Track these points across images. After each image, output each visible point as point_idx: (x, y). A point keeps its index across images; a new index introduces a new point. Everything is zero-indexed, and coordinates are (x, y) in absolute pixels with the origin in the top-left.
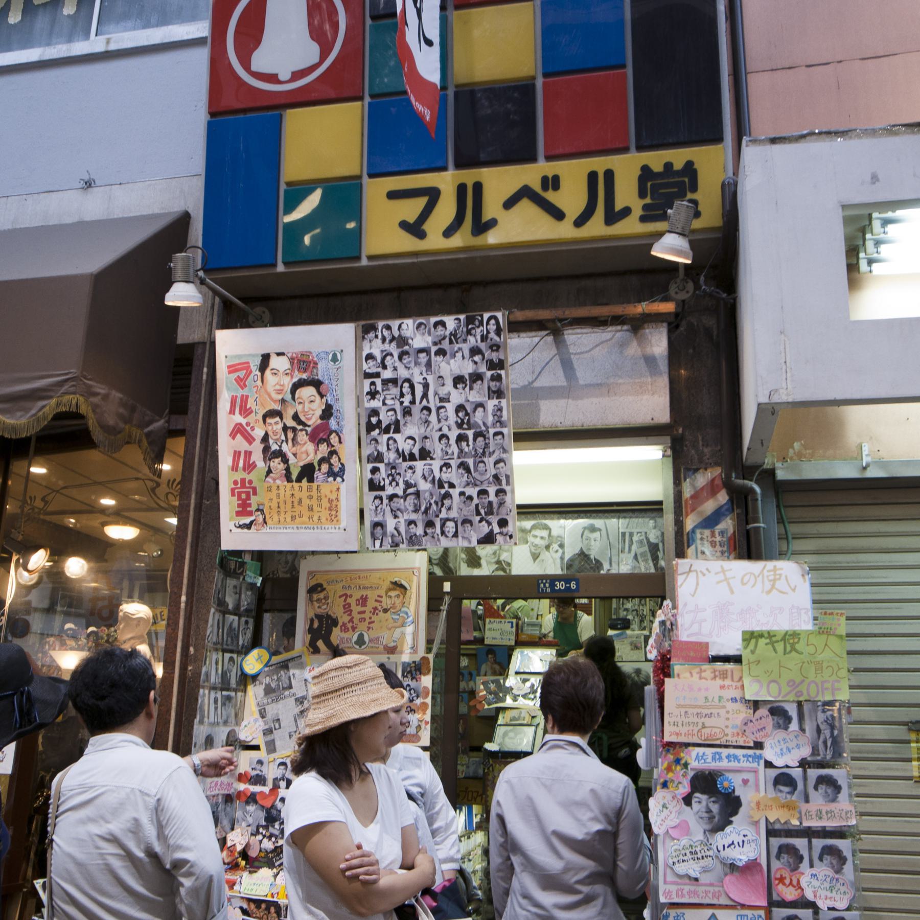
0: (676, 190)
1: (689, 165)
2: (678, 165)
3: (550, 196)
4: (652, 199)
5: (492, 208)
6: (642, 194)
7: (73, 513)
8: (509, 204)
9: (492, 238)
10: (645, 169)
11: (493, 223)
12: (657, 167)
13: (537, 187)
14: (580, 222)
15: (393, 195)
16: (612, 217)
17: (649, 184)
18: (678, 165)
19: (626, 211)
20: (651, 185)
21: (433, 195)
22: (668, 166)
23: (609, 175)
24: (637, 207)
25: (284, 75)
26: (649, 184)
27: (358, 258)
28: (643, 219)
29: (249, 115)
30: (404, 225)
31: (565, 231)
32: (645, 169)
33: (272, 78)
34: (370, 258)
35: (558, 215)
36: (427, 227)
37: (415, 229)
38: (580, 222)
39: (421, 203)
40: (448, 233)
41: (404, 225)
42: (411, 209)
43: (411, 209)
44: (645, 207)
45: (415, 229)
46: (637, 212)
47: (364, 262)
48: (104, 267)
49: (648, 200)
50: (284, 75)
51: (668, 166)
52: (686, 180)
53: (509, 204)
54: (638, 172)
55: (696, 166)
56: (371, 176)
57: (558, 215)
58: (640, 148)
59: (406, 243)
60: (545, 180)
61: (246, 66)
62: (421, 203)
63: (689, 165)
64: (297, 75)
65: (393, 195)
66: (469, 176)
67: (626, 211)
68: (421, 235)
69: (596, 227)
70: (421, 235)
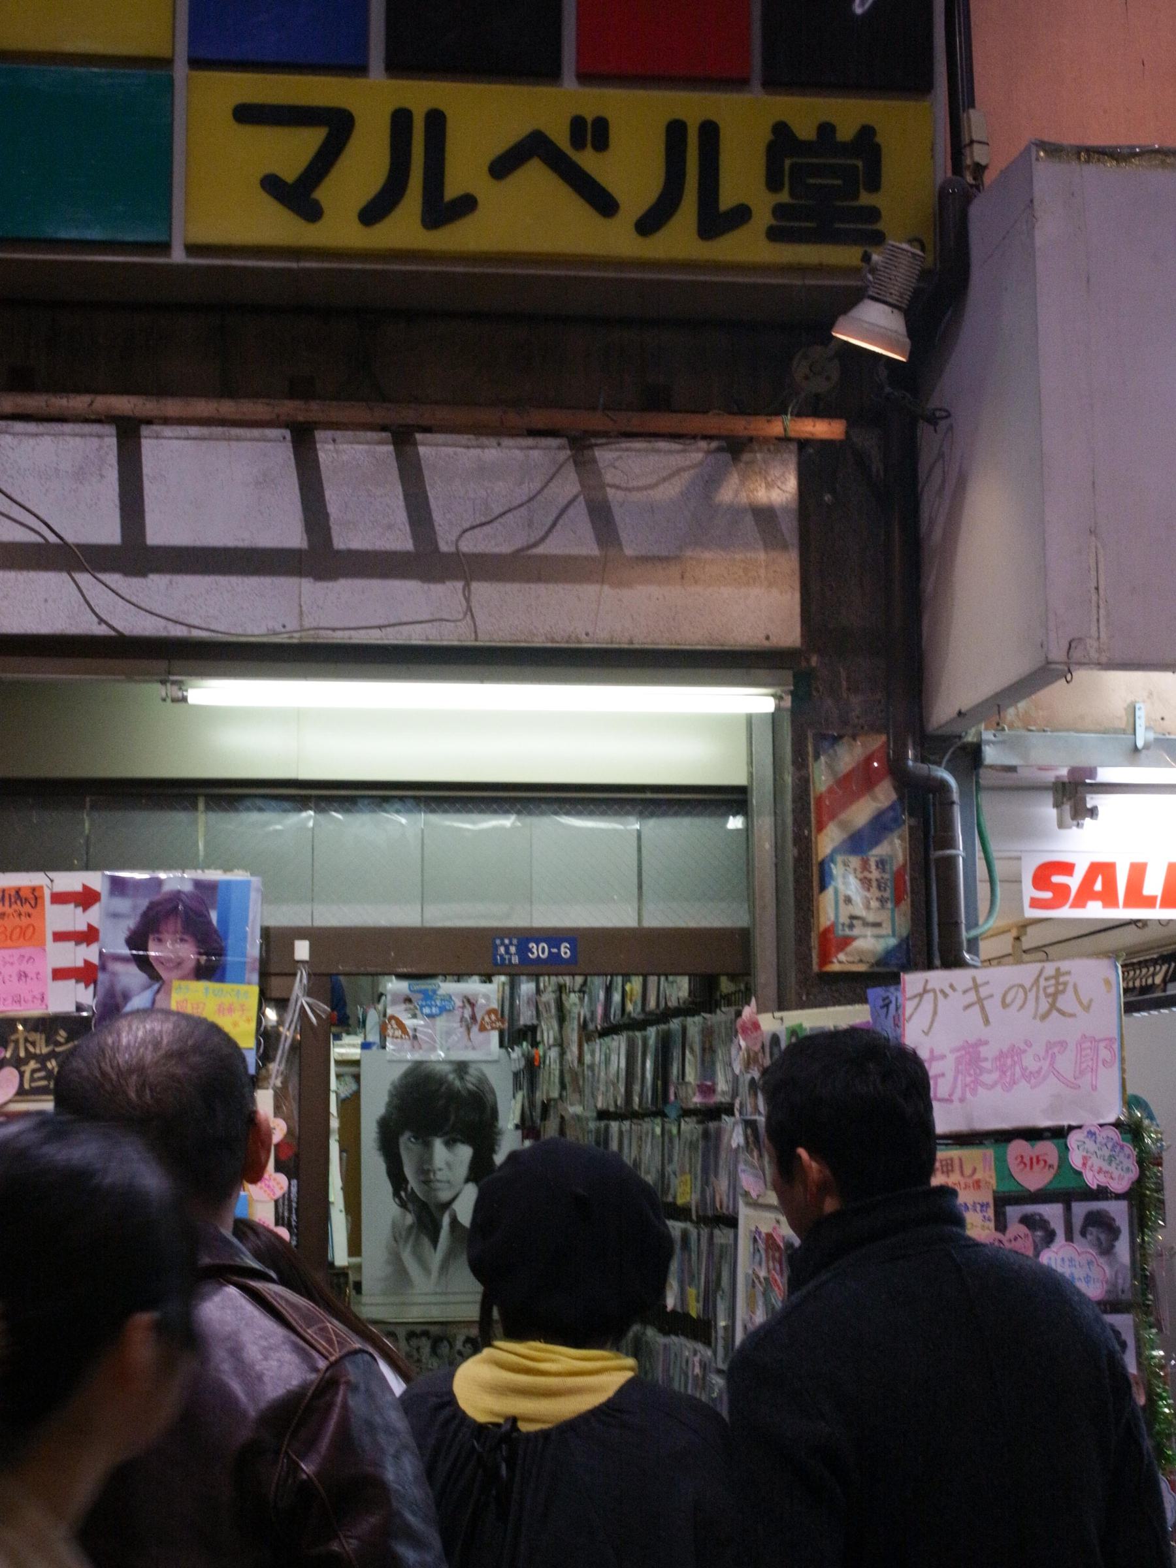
0: (839, 182)
1: (867, 132)
2: (846, 132)
3: (588, 160)
4: (792, 194)
6: (773, 183)
8: (502, 167)
10: (781, 130)
11: (467, 204)
12: (805, 131)
13: (561, 137)
14: (648, 224)
15: (247, 114)
17: (787, 163)
18: (846, 132)
19: (741, 214)
20: (792, 166)
22: (826, 130)
23: (710, 132)
24: (763, 205)
26: (787, 163)
27: (164, 247)
28: (774, 234)
30: (272, 185)
32: (781, 130)
34: (192, 249)
36: (323, 194)
38: (648, 224)
39: (311, 139)
40: (372, 214)
41: (272, 185)
44: (779, 211)
46: (762, 218)
47: (178, 256)
49: (784, 197)
51: (826, 130)
52: (860, 164)
53: (502, 167)
54: (768, 136)
55: (879, 139)
56: (196, 63)
58: (772, 84)
60: (578, 124)
62: (311, 139)
63: (867, 132)
65: (247, 114)
67: (741, 214)
68: (312, 213)
70: (312, 213)
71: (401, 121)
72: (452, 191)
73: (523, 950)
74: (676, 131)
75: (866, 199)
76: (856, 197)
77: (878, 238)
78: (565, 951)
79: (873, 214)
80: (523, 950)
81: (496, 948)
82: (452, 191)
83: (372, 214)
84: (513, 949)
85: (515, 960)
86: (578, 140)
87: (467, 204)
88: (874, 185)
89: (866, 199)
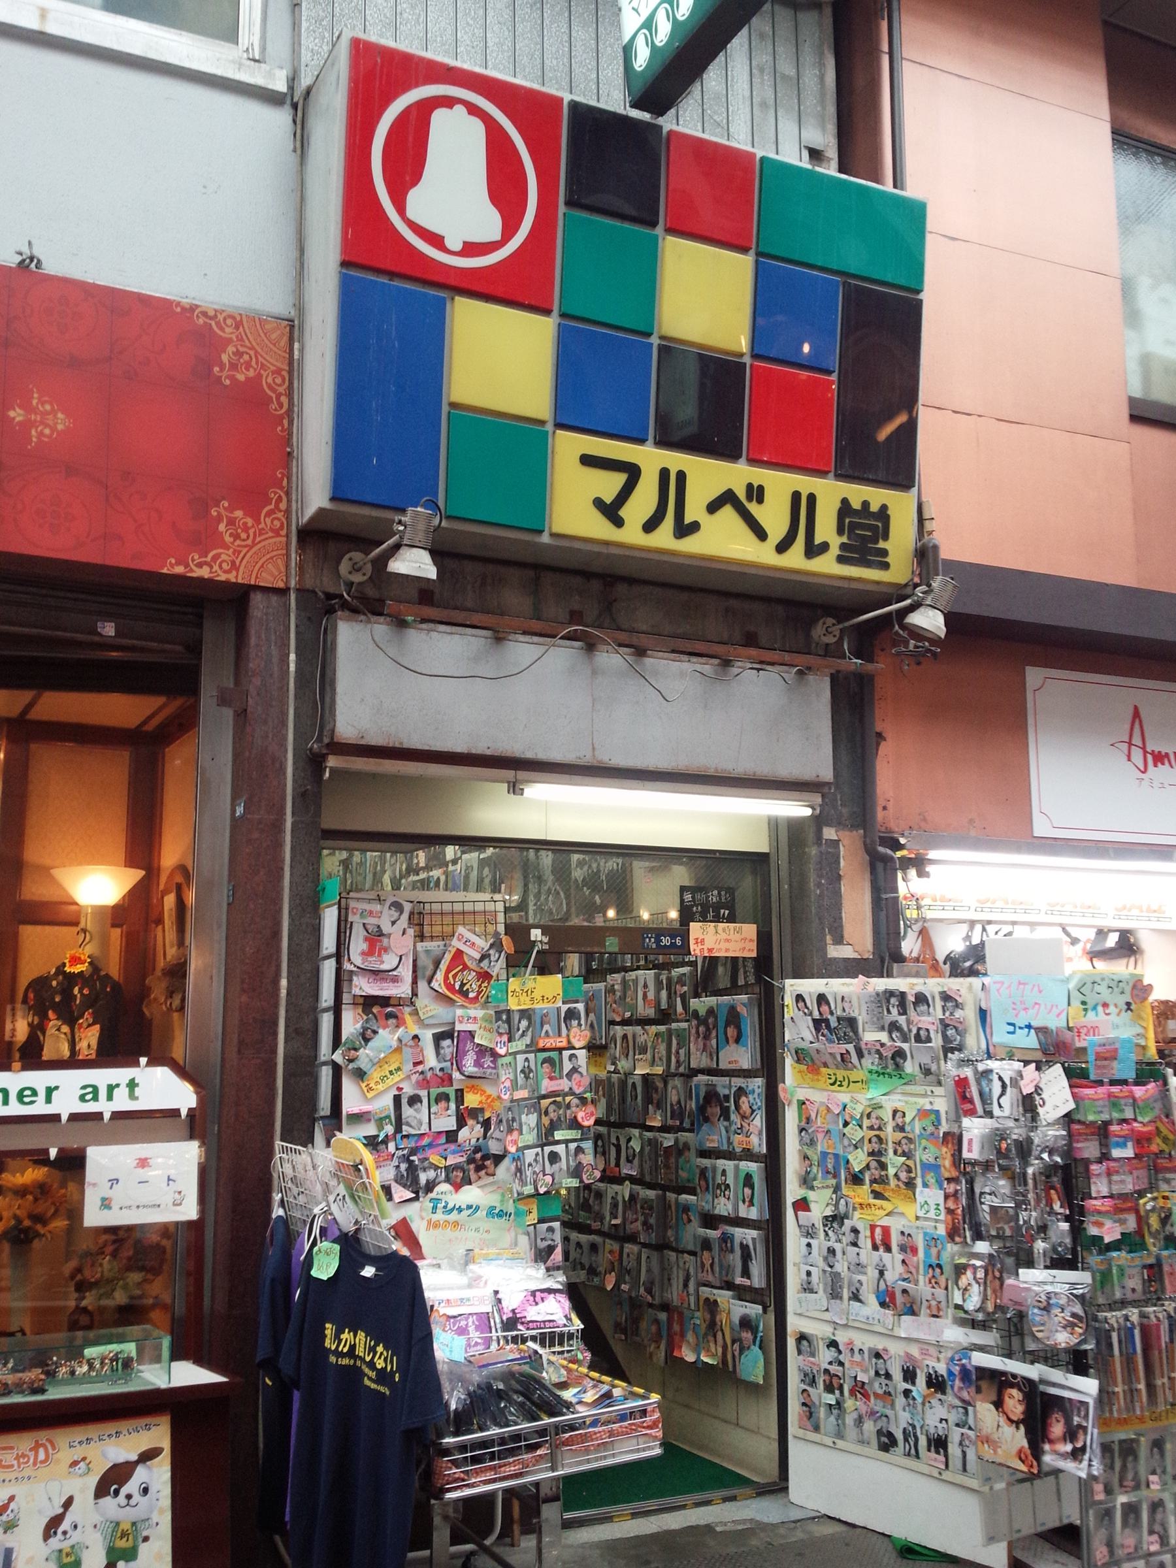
1: (884, 508)
2: (874, 507)
3: (753, 508)
4: (849, 538)
5: (694, 510)
6: (840, 531)
7: (289, 1295)
8: (713, 507)
9: (690, 545)
10: (845, 501)
11: (695, 527)
12: (856, 505)
13: (741, 494)
14: (782, 547)
15: (588, 461)
16: (813, 550)
17: (847, 520)
18: (874, 507)
19: (825, 547)
21: (633, 472)
22: (866, 504)
23: (812, 499)
25: (454, 244)
26: (847, 520)
27: (541, 532)
28: (841, 559)
29: (397, 283)
30: (599, 503)
31: (763, 554)
32: (845, 501)
33: (436, 241)
34: (552, 535)
35: (761, 534)
36: (622, 513)
37: (611, 511)
38: (783, 547)
39: (619, 479)
40: (650, 526)
41: (599, 503)
42: (609, 484)
43: (609, 484)
44: (843, 546)
45: (611, 511)
46: (834, 551)
47: (545, 539)
48: (342, 155)
49: (844, 539)
50: (454, 244)
51: (866, 504)
53: (713, 507)
54: (838, 505)
56: (559, 426)
57: (761, 534)
58: (840, 477)
59: (597, 528)
60: (750, 487)
61: (401, 209)
62: (619, 479)
63: (884, 508)
64: (471, 249)
65: (588, 461)
66: (676, 460)
67: (825, 547)
68: (618, 522)
69: (795, 558)
70: (618, 522)
71: (664, 474)
72: (688, 519)
73: (658, 941)
74: (796, 496)
75: (882, 545)
76: (877, 542)
77: (885, 566)
79: (884, 553)
80: (658, 941)
82: (688, 519)
83: (650, 526)
85: (654, 946)
86: (749, 498)
87: (695, 527)
88: (886, 537)
89: (882, 545)
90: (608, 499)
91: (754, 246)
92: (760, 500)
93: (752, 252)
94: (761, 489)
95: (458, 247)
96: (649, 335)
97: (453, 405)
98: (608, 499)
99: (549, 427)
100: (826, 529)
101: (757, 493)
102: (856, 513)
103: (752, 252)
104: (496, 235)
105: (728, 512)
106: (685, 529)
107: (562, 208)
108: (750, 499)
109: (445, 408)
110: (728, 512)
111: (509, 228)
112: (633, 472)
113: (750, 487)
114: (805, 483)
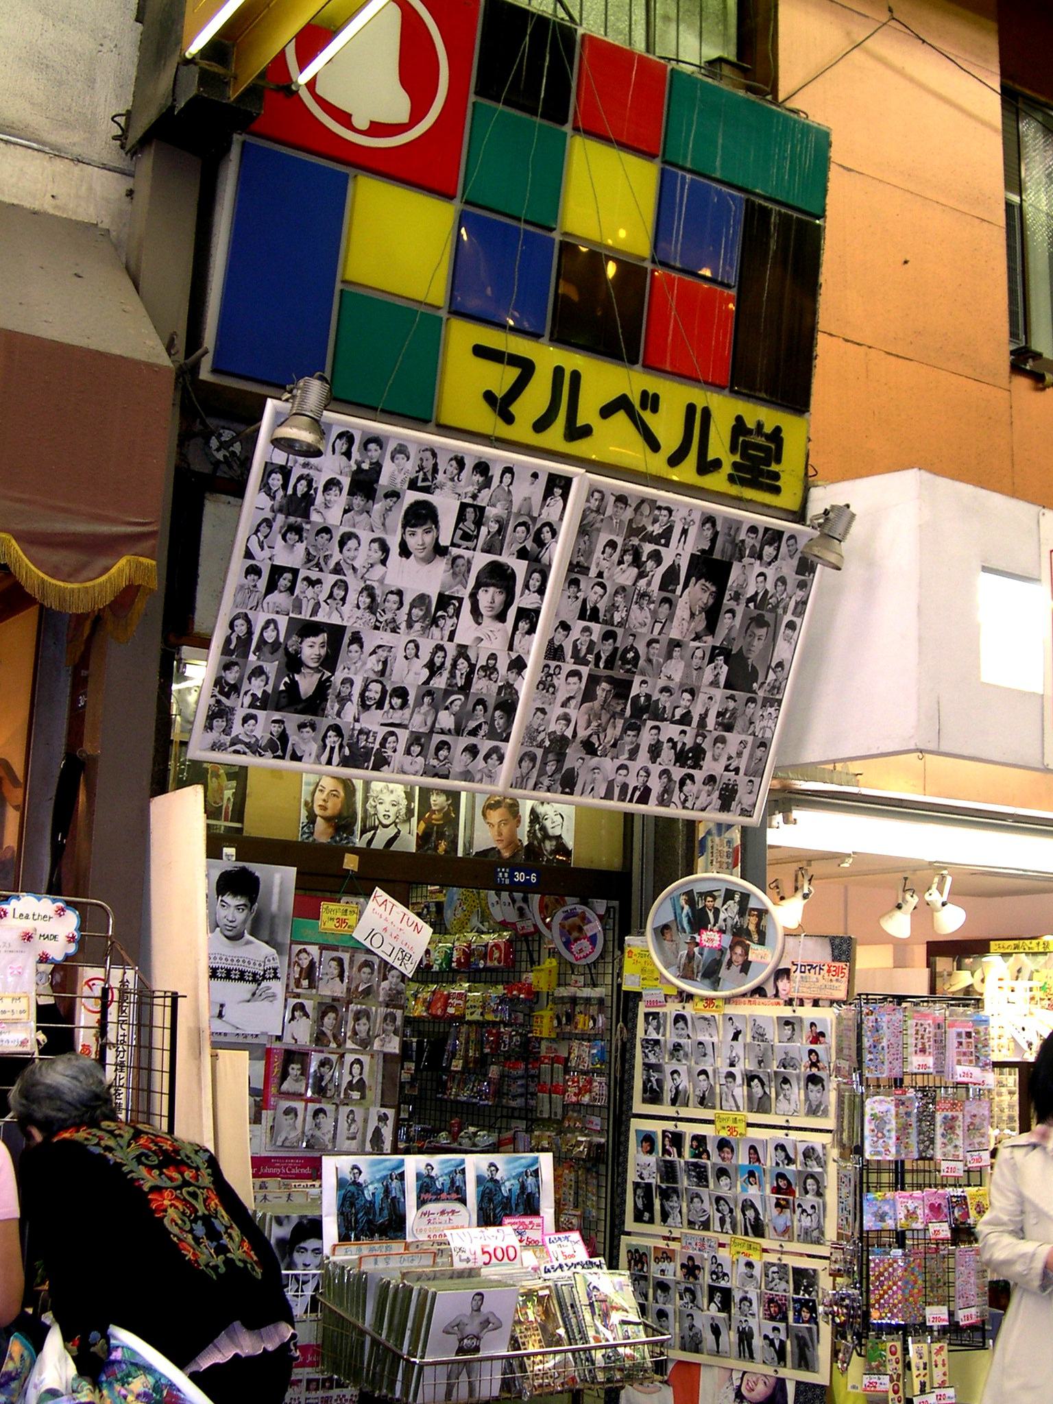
0: (762, 455)
1: (778, 430)
3: (647, 416)
4: (741, 458)
5: (587, 414)
6: (733, 450)
8: (607, 412)
10: (739, 419)
11: (587, 431)
12: (751, 424)
13: (636, 400)
15: (481, 352)
16: (707, 466)
17: (741, 439)
19: (717, 464)
20: (743, 441)
23: (706, 413)
25: (361, 122)
26: (741, 439)
30: (489, 397)
32: (739, 419)
33: (344, 118)
36: (513, 409)
38: (675, 460)
39: (513, 373)
40: (541, 425)
41: (489, 397)
42: (501, 378)
43: (501, 378)
44: (735, 465)
45: (502, 405)
46: (727, 469)
49: (737, 458)
50: (361, 122)
51: (760, 426)
52: (773, 447)
53: (607, 412)
55: (782, 435)
58: (735, 393)
60: (644, 394)
62: (513, 373)
63: (778, 430)
64: (377, 129)
65: (481, 352)
66: (573, 360)
67: (717, 464)
68: (509, 419)
70: (509, 419)
71: (559, 371)
72: (580, 422)
74: (691, 409)
75: (774, 467)
76: (769, 465)
77: (776, 490)
78: (533, 878)
79: (776, 476)
80: (512, 876)
81: (498, 873)
82: (580, 422)
83: (541, 425)
84: (506, 875)
85: (507, 882)
86: (644, 406)
87: (587, 431)
88: (778, 461)
89: (774, 467)
90: (500, 392)
91: (661, 153)
92: (655, 410)
93: (658, 160)
94: (656, 398)
95: (364, 126)
96: (552, 230)
97: (344, 282)
98: (500, 392)
99: (443, 314)
100: (719, 446)
101: (651, 401)
102: (749, 432)
103: (658, 160)
104: (403, 117)
105: (621, 417)
106: (577, 432)
107: (472, 98)
108: (644, 407)
109: (338, 286)
110: (621, 417)
111: (418, 113)
112: (527, 368)
113: (644, 394)
114: (701, 397)
